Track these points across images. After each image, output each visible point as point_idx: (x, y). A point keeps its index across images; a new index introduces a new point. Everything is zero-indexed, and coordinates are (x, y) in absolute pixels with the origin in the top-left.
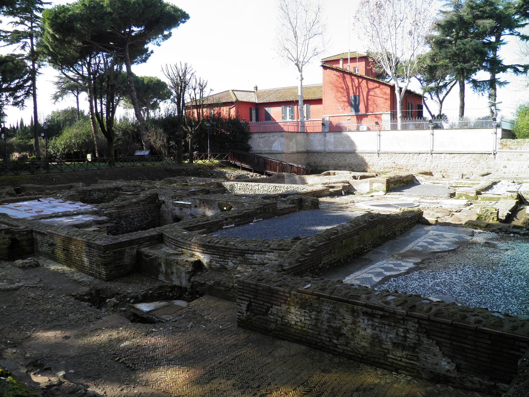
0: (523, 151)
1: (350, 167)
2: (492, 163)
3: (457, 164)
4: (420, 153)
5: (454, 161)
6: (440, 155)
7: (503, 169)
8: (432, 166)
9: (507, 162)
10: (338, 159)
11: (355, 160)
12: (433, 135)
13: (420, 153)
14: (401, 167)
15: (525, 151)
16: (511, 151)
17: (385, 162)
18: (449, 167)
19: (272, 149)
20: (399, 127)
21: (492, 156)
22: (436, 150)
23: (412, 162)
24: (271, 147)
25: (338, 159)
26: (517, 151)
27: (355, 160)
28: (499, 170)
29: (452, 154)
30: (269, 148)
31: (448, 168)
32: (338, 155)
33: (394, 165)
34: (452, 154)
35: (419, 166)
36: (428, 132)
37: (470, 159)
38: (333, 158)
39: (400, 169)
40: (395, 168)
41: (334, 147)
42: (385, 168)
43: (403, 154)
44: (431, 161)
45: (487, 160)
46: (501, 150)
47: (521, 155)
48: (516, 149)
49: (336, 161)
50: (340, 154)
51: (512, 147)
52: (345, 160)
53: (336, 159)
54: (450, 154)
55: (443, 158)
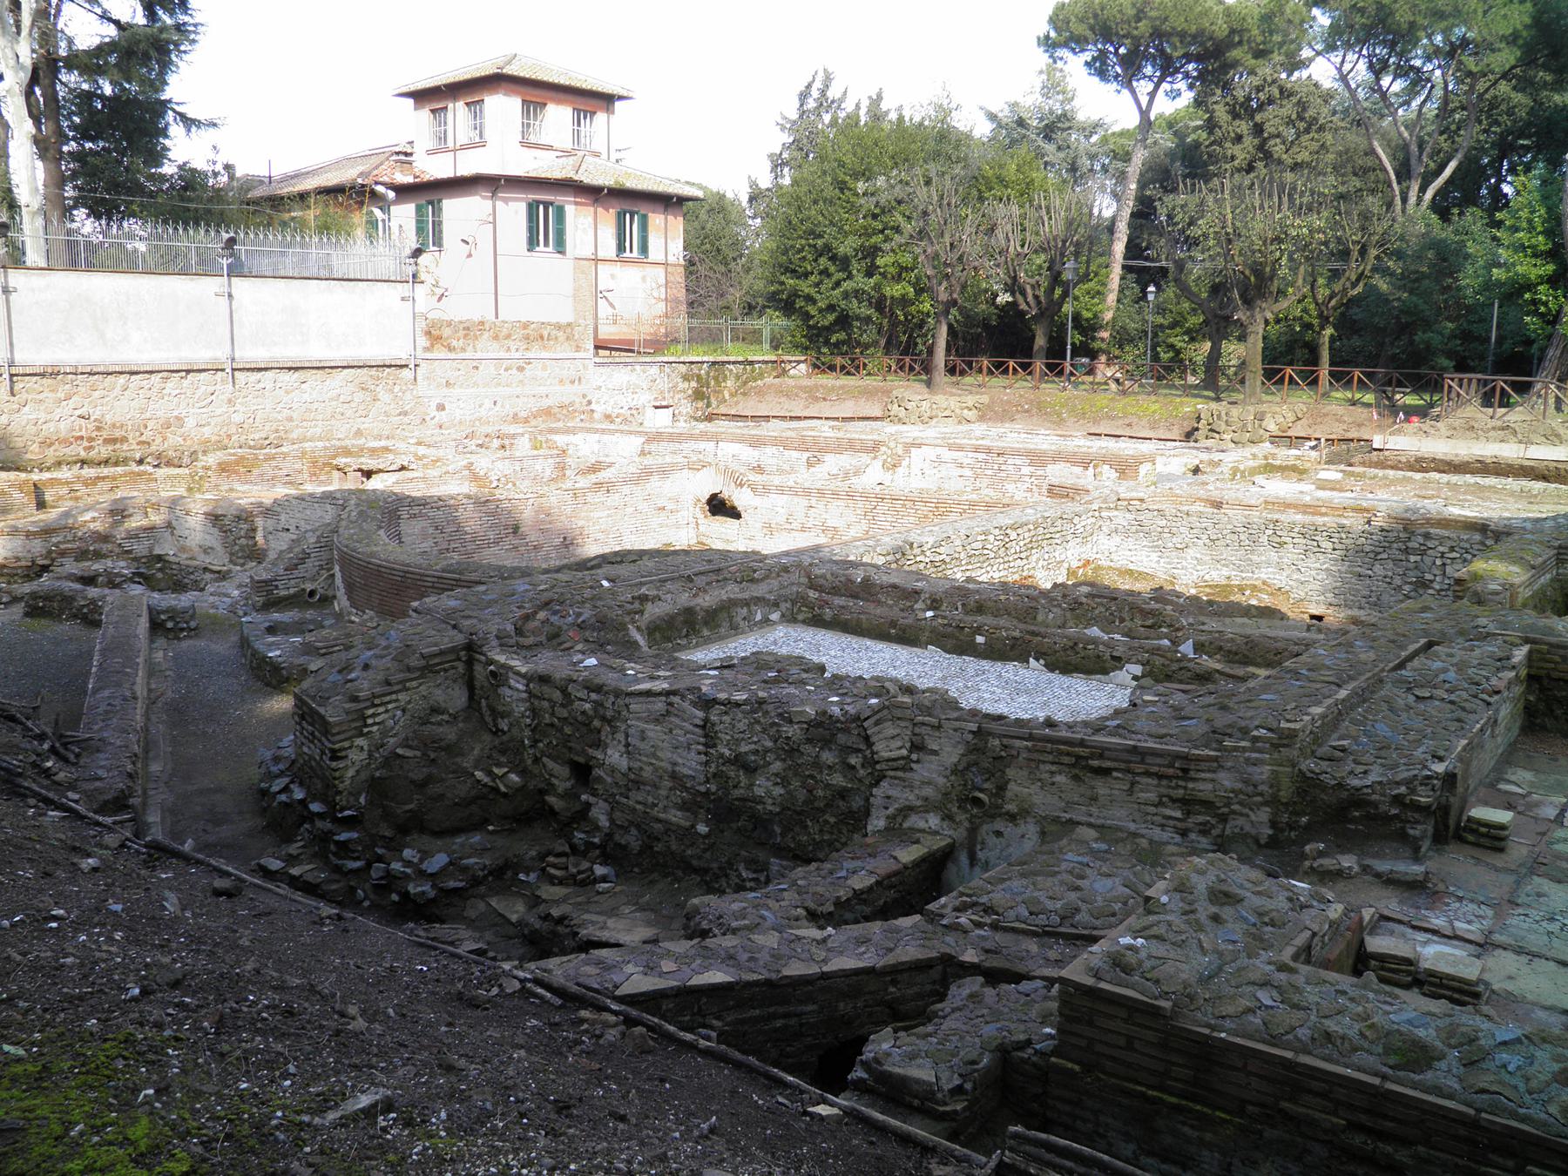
0: (478, 355)
2: (408, 396)
3: (316, 405)
4: (188, 372)
5: (306, 397)
6: (259, 375)
7: (436, 413)
8: (237, 418)
12: (230, 296)
13: (188, 372)
14: (118, 434)
15: (485, 355)
16: (452, 356)
17: (43, 416)
18: (290, 419)
20: (34, 256)
21: (406, 374)
22: (249, 353)
23: (161, 410)
28: (428, 418)
29: (297, 369)
31: (289, 425)
33: (86, 428)
34: (297, 369)
35: (190, 423)
36: (209, 287)
37: (351, 387)
39: (114, 441)
40: (91, 439)
42: (46, 443)
43: (122, 379)
44: (230, 401)
45: (397, 389)
46: (429, 355)
47: (477, 368)
48: (463, 350)
51: (454, 343)
54: (290, 369)
55: (269, 386)
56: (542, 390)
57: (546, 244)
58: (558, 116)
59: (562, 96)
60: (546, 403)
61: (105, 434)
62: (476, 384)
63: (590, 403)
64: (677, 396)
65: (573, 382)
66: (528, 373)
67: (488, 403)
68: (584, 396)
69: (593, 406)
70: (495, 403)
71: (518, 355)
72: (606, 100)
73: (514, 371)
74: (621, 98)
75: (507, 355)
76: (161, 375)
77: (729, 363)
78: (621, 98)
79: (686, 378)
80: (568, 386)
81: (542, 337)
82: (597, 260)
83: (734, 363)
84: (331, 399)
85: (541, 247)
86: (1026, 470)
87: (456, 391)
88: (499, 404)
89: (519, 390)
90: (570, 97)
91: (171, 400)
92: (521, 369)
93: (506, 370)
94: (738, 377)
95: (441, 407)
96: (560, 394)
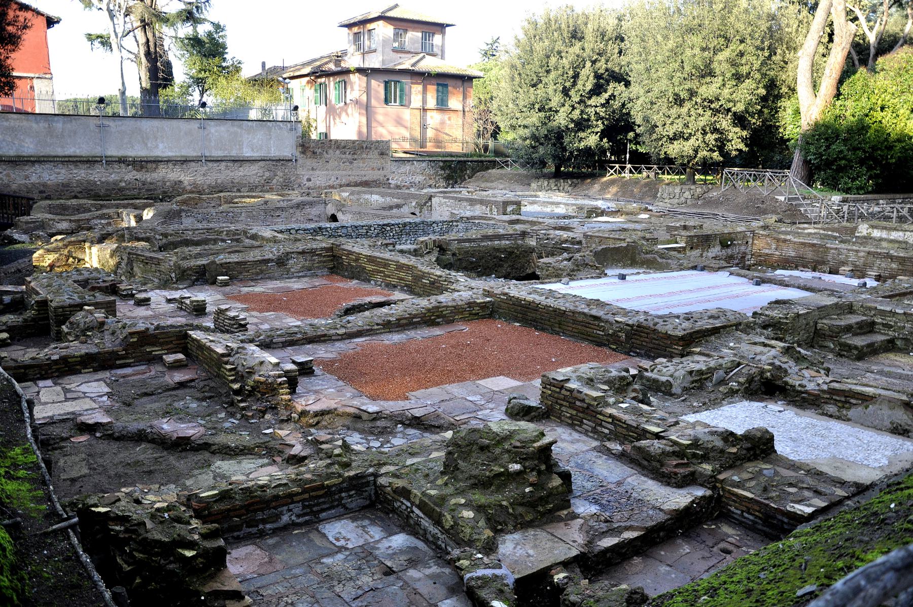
25: (8, 175)
27: (52, 178)
39: (151, 190)
40: (140, 189)
44: (204, 174)
57: (395, 102)
58: (413, 37)
59: (416, 25)
60: (364, 179)
61: (146, 187)
62: (327, 170)
63: (388, 179)
64: (437, 178)
65: (379, 169)
67: (333, 179)
68: (385, 176)
69: (390, 181)
72: (441, 27)
74: (448, 25)
77: (468, 161)
78: (448, 25)
79: (442, 168)
80: (376, 172)
81: (363, 147)
82: (424, 110)
83: (471, 161)
84: (254, 175)
85: (393, 104)
86: (468, 208)
87: (317, 172)
88: (339, 179)
89: (350, 173)
90: (420, 26)
91: (173, 175)
92: (351, 163)
93: (343, 163)
94: (473, 169)
96: (370, 175)
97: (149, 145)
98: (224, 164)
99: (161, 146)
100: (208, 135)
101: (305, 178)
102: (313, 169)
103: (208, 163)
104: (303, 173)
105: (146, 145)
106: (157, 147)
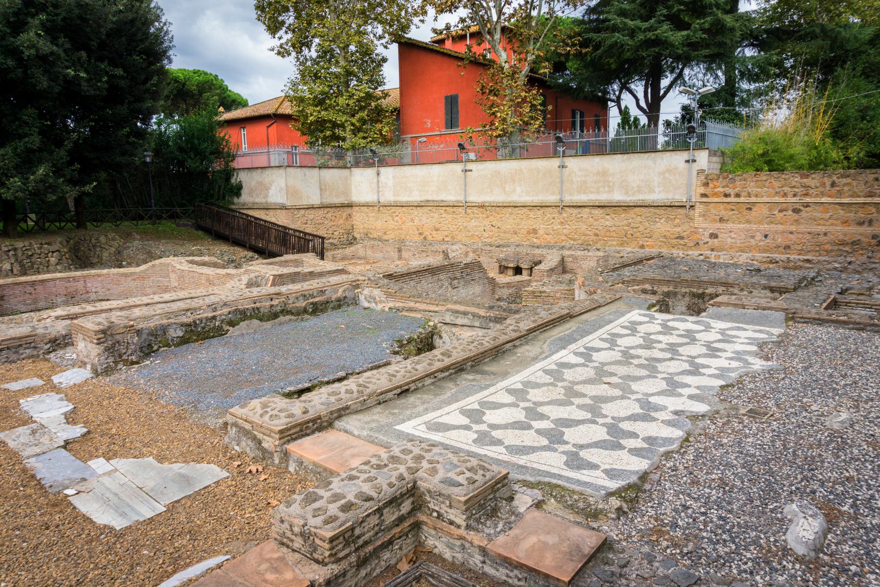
1: (420, 234)
6: (579, 210)
7: (709, 240)
9: (718, 225)
10: (401, 218)
11: (428, 221)
19: (269, 201)
24: (266, 196)
25: (401, 218)
26: (742, 199)
27: (428, 221)
28: (701, 243)
30: (264, 198)
32: (400, 210)
35: (541, 232)
36: (555, 163)
38: (392, 217)
41: (394, 195)
43: (510, 210)
49: (397, 221)
50: (404, 209)
52: (412, 220)
53: (396, 218)
54: (599, 207)
56: (822, 229)
62: (748, 222)
66: (804, 214)
67: (759, 236)
70: (766, 236)
71: (794, 200)
73: (790, 212)
75: (782, 200)
76: (429, 208)
87: (730, 225)
88: (771, 236)
89: (793, 228)
92: (796, 211)
95: (714, 236)
97: (507, 189)
98: (587, 210)
99: (519, 190)
100: (570, 175)
101: (707, 234)
102: (721, 220)
103: (566, 209)
104: (704, 226)
105: (504, 189)
106: (514, 191)
